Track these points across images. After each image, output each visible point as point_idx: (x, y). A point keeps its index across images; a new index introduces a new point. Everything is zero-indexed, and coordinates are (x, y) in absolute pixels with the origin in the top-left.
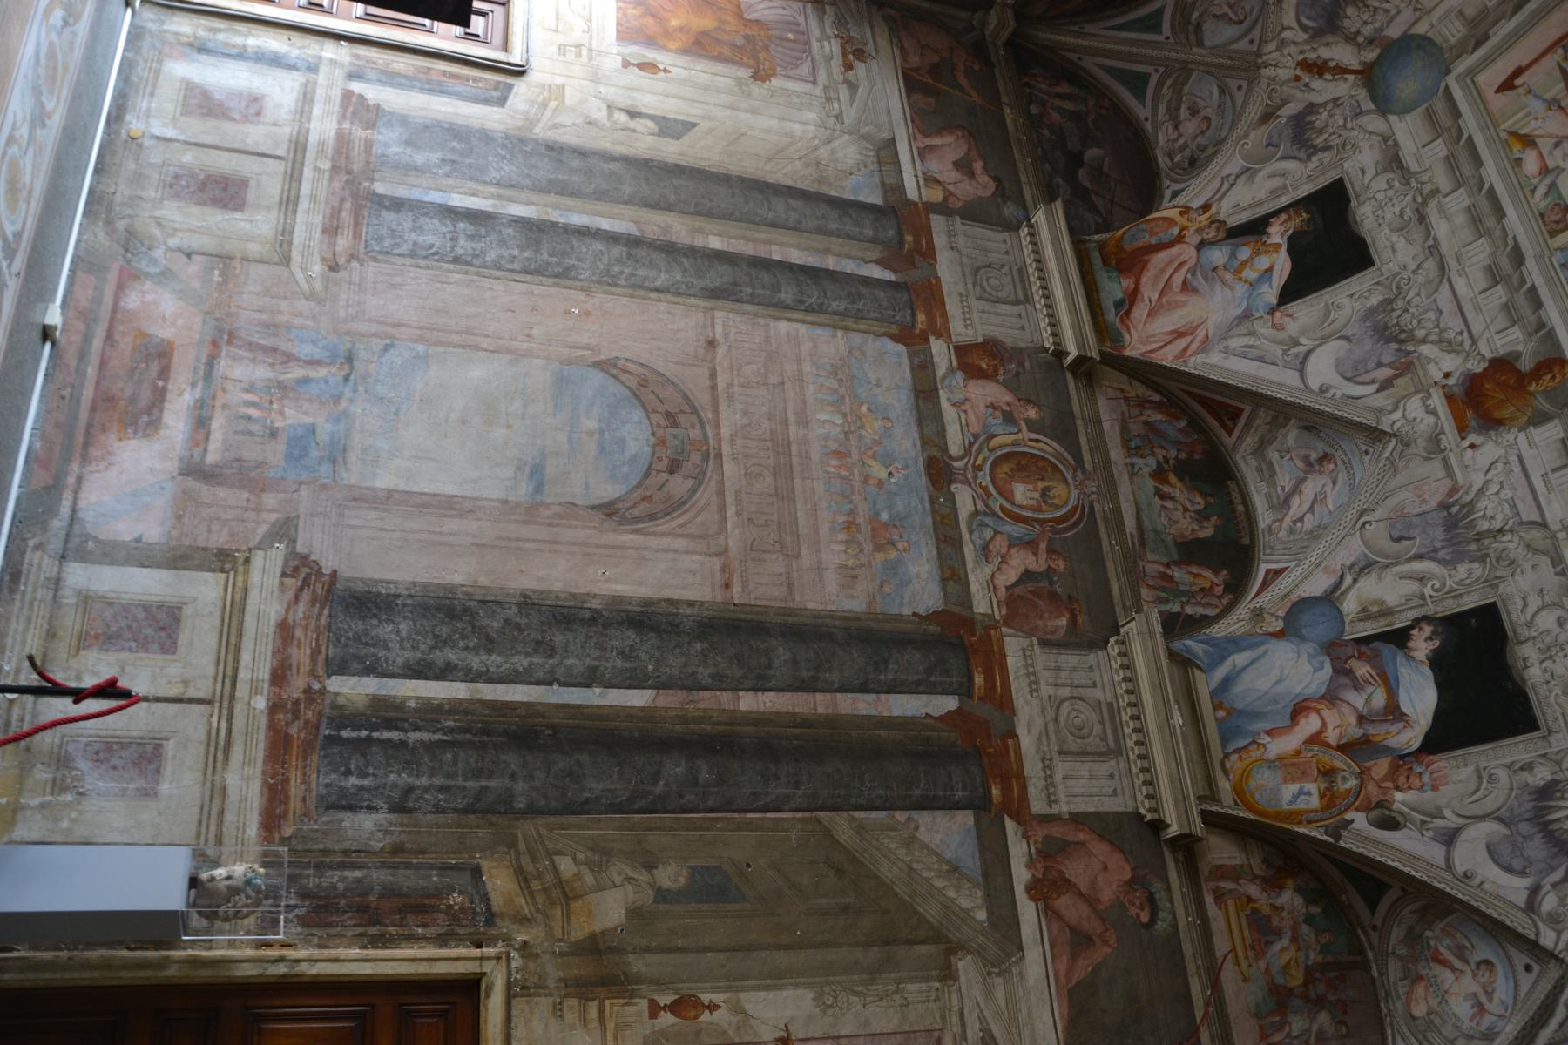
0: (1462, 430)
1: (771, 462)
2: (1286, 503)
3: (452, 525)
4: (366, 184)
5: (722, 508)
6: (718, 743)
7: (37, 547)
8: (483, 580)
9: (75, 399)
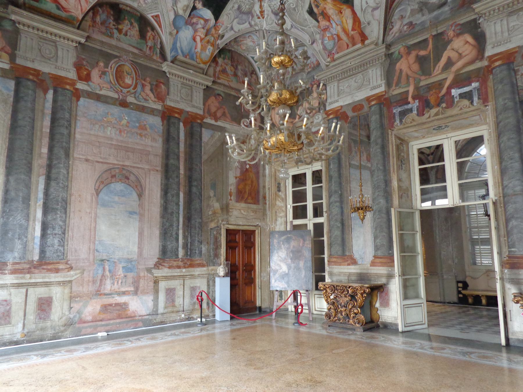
1: (124, 152)
3: (146, 233)
4: (35, 262)
5: (138, 168)
6: (190, 179)
7: (155, 320)
8: (158, 226)
9: (119, 323)
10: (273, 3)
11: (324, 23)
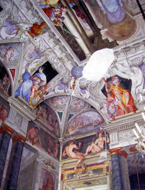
0: (33, 37)
2: (5, 56)
10: (82, 82)
11: (110, 98)
